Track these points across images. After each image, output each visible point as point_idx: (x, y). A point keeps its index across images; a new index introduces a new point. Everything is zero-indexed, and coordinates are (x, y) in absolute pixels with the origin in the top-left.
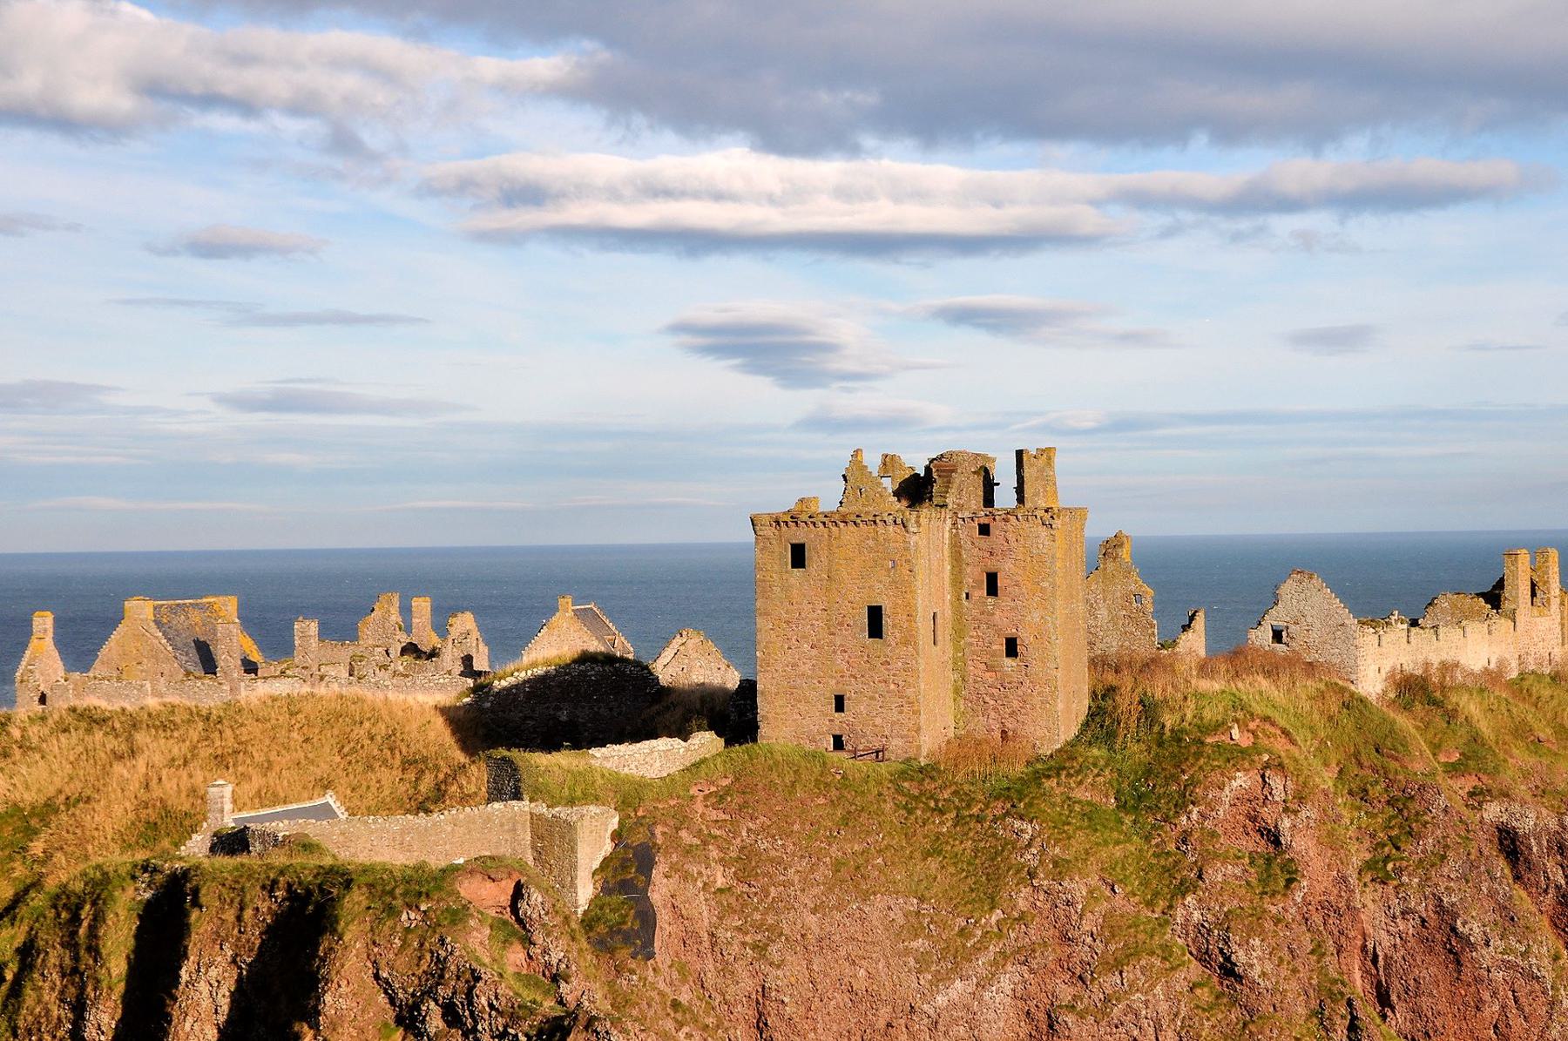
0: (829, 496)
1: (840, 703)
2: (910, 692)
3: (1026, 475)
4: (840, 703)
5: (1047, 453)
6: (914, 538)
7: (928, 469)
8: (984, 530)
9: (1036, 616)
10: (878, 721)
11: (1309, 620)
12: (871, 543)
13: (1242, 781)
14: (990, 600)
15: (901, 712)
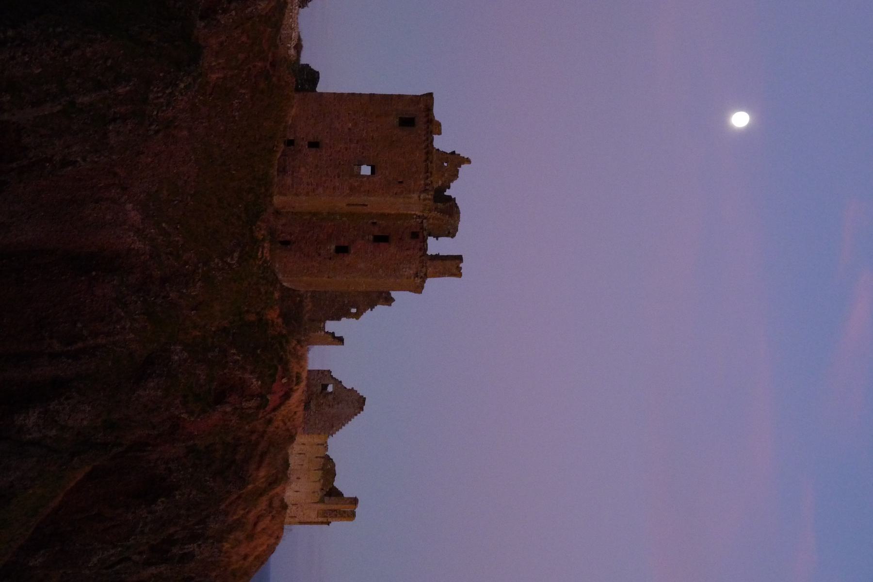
0: (441, 143)
1: (314, 145)
2: (321, 190)
3: (448, 263)
4: (314, 145)
5: (458, 273)
6: (415, 196)
7: (450, 199)
8: (415, 235)
9: (362, 265)
10: (303, 170)
11: (336, 406)
12: (414, 169)
13: (256, 384)
14: (371, 237)
15: (308, 184)
